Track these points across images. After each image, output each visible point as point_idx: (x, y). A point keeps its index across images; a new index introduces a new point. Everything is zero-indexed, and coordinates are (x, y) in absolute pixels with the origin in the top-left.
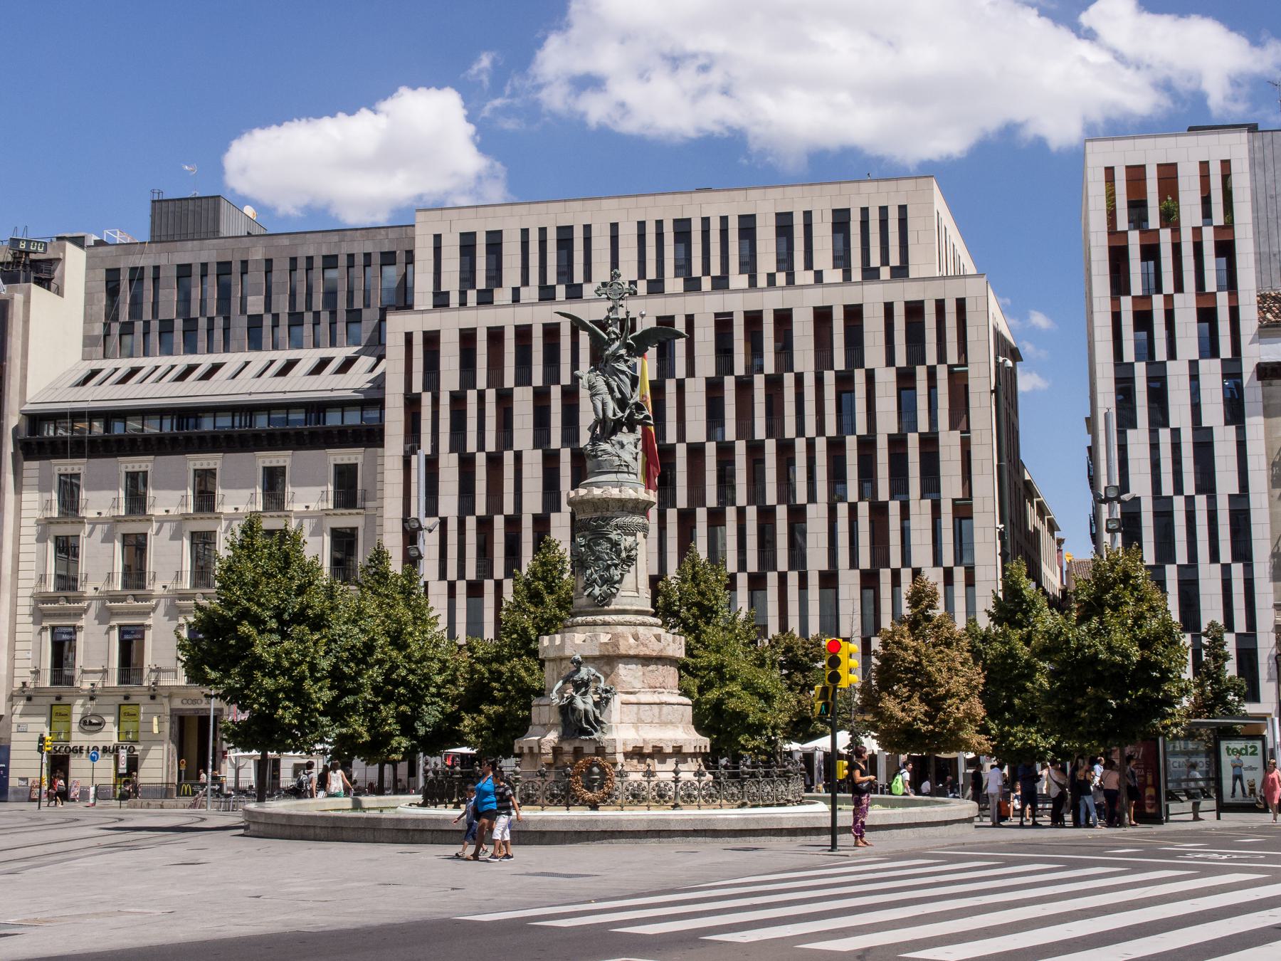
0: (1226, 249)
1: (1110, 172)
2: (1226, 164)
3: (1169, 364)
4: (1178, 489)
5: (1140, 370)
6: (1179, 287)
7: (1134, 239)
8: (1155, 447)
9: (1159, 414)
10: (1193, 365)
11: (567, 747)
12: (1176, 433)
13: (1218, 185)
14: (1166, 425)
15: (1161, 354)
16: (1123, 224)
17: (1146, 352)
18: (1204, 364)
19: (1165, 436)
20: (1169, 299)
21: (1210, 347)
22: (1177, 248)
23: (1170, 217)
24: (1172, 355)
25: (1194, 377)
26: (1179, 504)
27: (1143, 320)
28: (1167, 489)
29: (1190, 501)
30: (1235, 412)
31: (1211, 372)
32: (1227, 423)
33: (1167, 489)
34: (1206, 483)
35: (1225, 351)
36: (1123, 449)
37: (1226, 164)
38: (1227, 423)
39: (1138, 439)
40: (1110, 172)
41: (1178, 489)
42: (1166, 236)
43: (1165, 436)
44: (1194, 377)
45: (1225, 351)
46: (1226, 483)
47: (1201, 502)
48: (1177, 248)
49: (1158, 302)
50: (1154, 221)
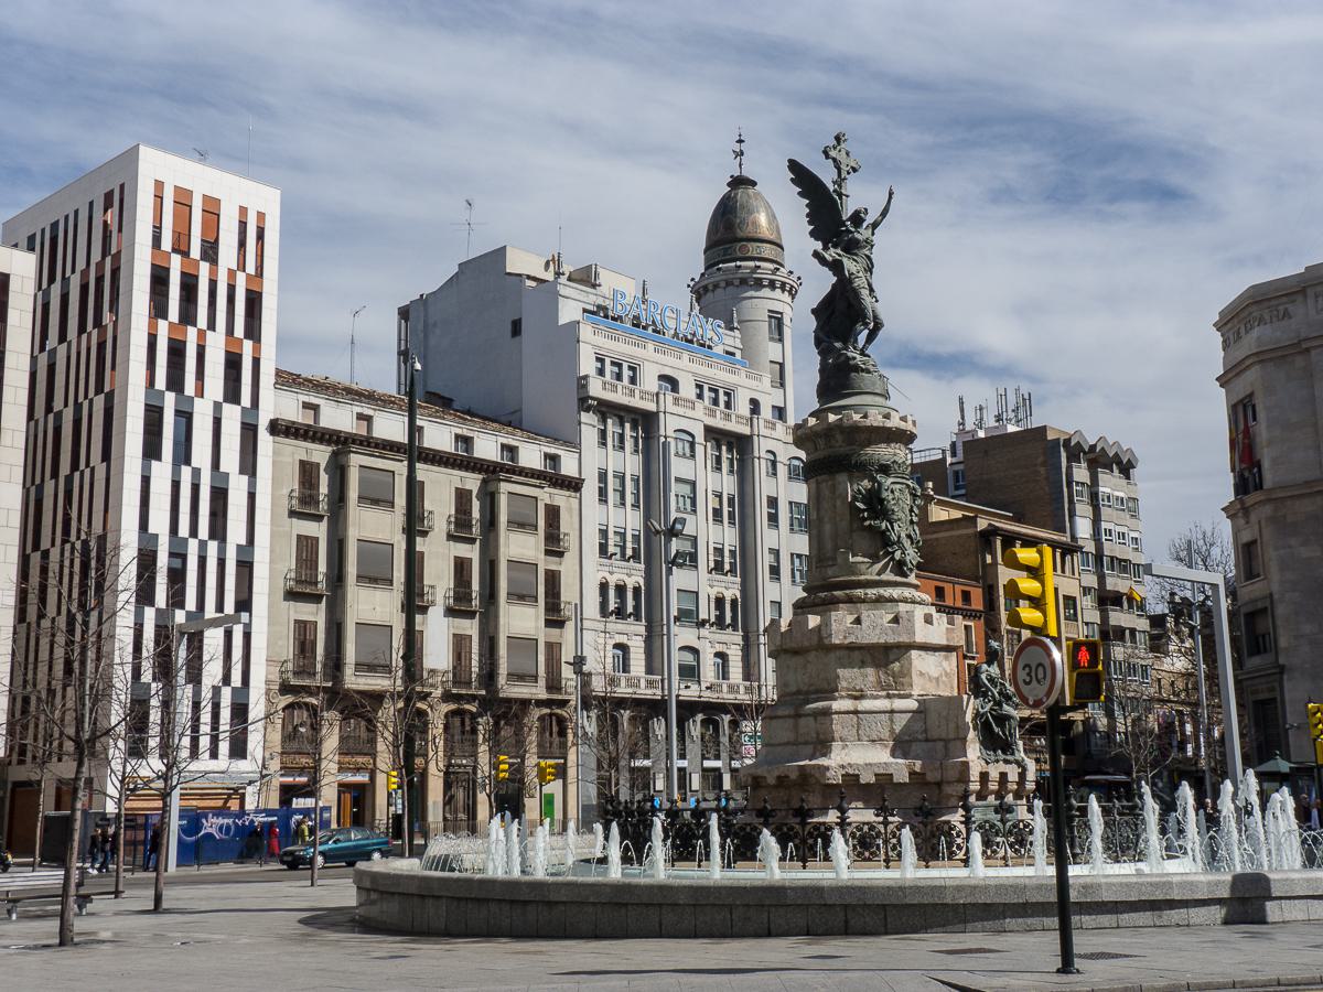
0: (254, 301)
1: (159, 185)
2: (261, 216)
3: (197, 401)
4: (194, 532)
5: (170, 400)
6: (212, 326)
7: (176, 265)
8: (176, 485)
9: (183, 454)
10: (217, 406)
11: (994, 774)
12: (196, 473)
13: (251, 233)
14: (188, 462)
15: (190, 389)
16: (167, 245)
17: (176, 383)
18: (226, 407)
19: (186, 472)
20: (202, 334)
21: (232, 394)
22: (213, 284)
23: (211, 251)
24: (200, 392)
25: (217, 422)
26: (193, 548)
27: (177, 351)
28: (184, 531)
29: (203, 545)
30: (249, 466)
31: (232, 417)
32: (241, 472)
33: (184, 531)
34: (218, 531)
35: (246, 400)
36: (146, 481)
37: (261, 216)
38: (241, 472)
39: (162, 471)
40: (159, 185)
41: (194, 532)
42: (204, 269)
43: (186, 472)
44: (217, 422)
45: (246, 400)
46: (236, 533)
47: (213, 546)
48: (213, 284)
49: (192, 333)
50: (195, 253)
